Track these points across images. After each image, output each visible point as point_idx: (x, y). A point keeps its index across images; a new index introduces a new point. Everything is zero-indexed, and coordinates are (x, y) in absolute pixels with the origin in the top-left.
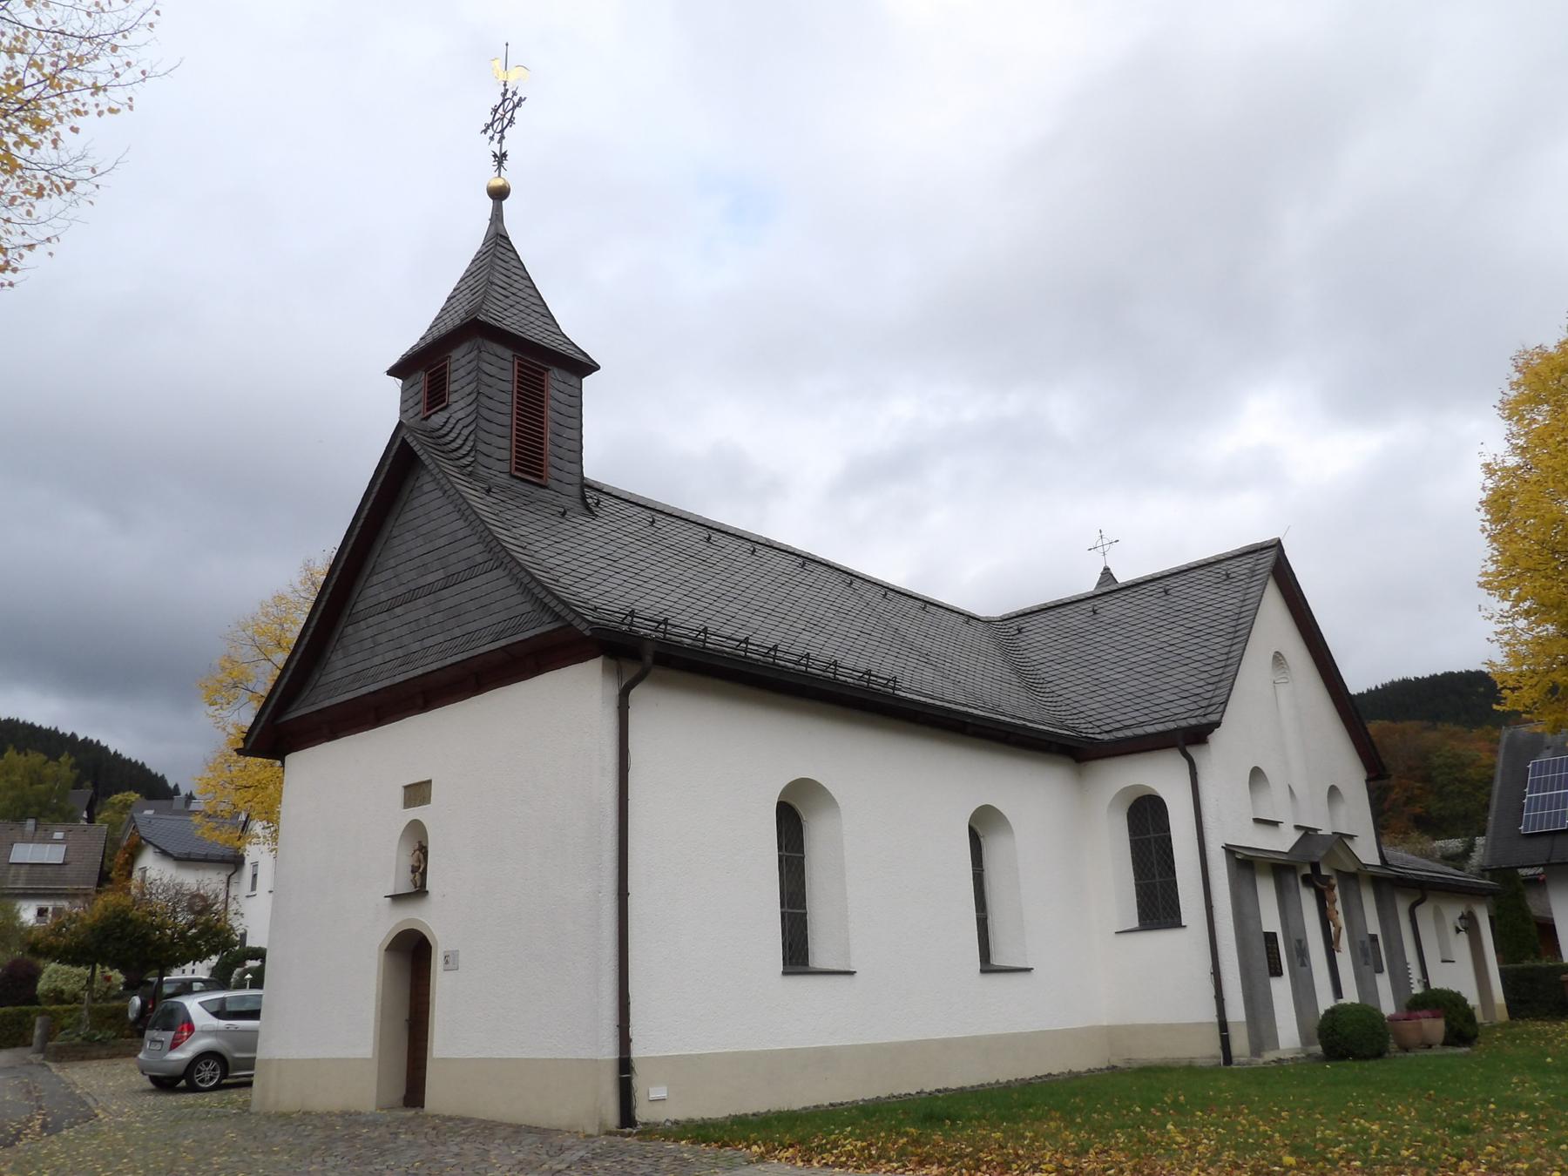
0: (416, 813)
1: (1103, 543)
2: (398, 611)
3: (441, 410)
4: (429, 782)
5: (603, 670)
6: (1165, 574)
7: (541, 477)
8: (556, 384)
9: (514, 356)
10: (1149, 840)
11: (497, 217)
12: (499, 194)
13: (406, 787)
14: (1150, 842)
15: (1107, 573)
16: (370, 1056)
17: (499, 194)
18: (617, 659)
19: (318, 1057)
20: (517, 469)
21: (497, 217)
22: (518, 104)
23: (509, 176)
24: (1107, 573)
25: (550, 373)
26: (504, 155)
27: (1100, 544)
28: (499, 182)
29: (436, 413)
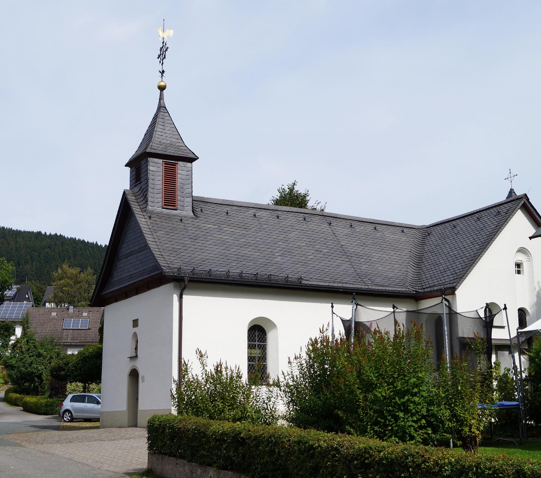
0: (136, 330)
1: (511, 176)
2: (129, 258)
3: (139, 183)
4: (138, 319)
5: (174, 287)
6: (490, 207)
7: (175, 206)
8: (181, 168)
9: (163, 161)
10: (255, 344)
11: (161, 98)
12: (162, 88)
13: (133, 321)
14: (255, 346)
15: (511, 192)
16: (126, 410)
17: (162, 88)
18: (179, 282)
19: (115, 410)
20: (165, 205)
21: (161, 98)
22: (166, 50)
23: (166, 81)
24: (511, 192)
25: (179, 164)
26: (163, 72)
27: (509, 176)
28: (162, 84)
29: (138, 184)
